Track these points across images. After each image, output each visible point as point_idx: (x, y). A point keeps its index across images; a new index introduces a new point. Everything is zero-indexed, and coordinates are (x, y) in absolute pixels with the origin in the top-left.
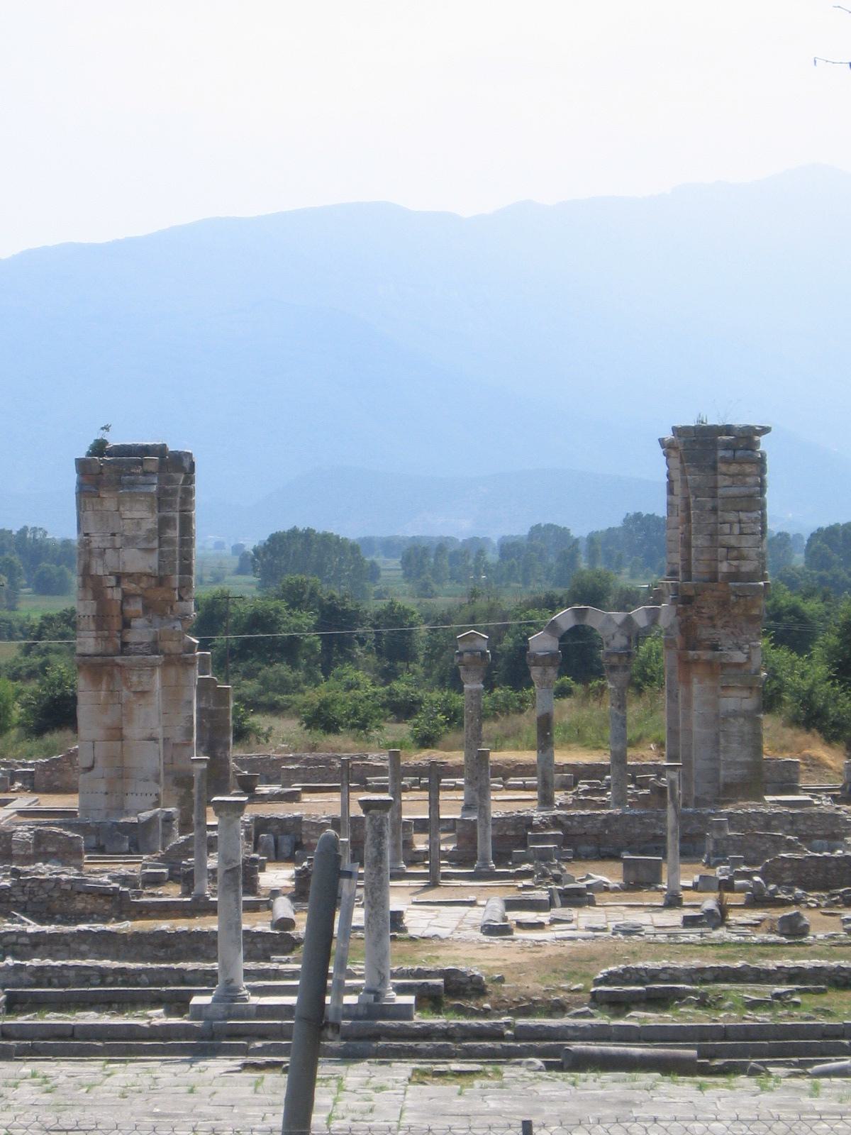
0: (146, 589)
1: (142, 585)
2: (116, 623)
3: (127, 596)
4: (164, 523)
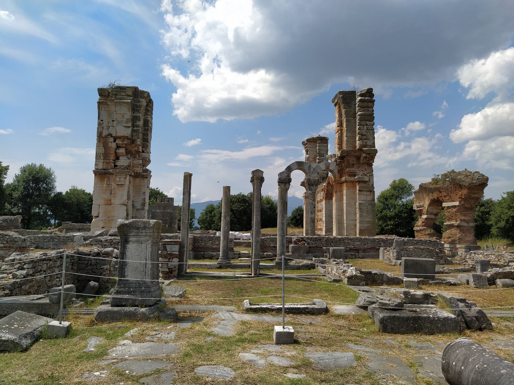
0: (126, 144)
1: (124, 142)
2: (112, 157)
3: (118, 147)
4: (134, 119)
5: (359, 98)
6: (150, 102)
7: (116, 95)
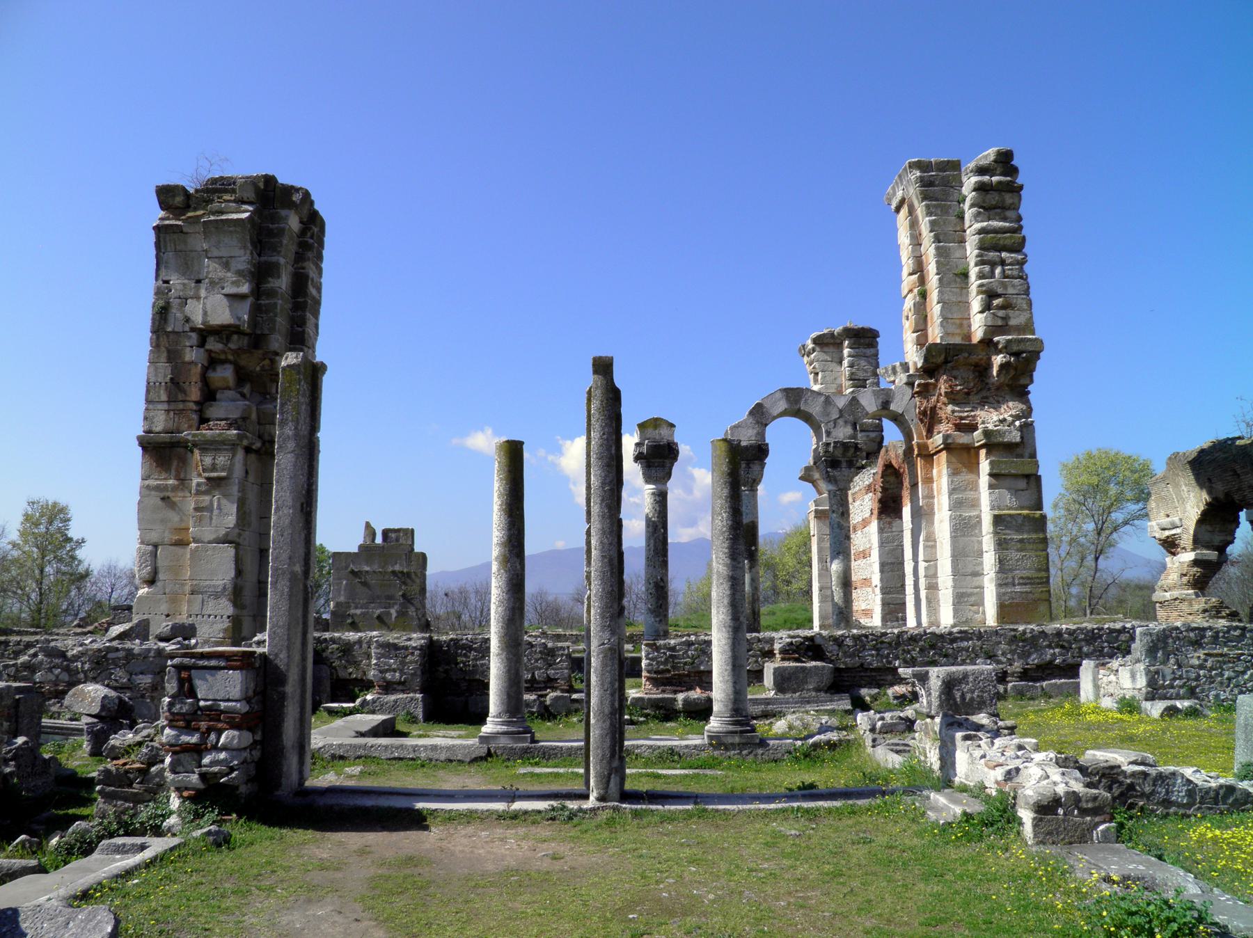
0: (236, 352)
1: (232, 346)
2: (195, 393)
3: (213, 361)
5: (974, 179)
6: (313, 223)
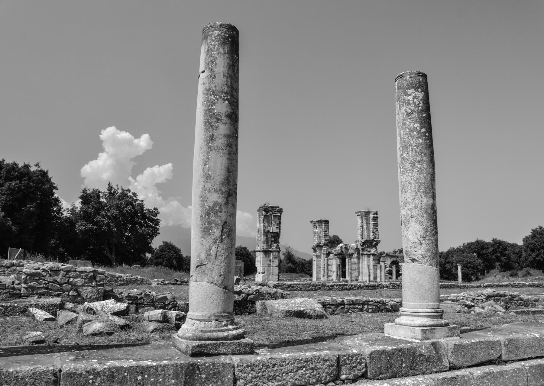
2: (270, 243)
7: (272, 211)
